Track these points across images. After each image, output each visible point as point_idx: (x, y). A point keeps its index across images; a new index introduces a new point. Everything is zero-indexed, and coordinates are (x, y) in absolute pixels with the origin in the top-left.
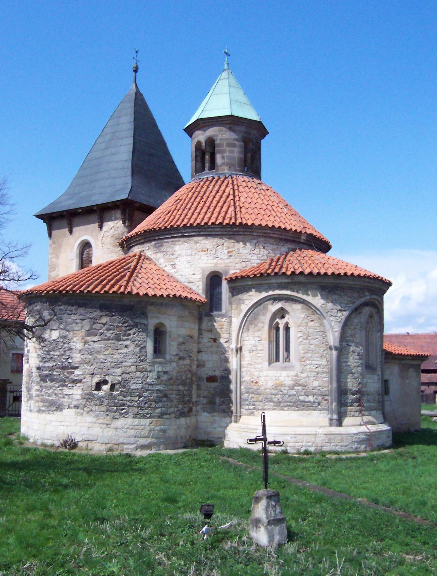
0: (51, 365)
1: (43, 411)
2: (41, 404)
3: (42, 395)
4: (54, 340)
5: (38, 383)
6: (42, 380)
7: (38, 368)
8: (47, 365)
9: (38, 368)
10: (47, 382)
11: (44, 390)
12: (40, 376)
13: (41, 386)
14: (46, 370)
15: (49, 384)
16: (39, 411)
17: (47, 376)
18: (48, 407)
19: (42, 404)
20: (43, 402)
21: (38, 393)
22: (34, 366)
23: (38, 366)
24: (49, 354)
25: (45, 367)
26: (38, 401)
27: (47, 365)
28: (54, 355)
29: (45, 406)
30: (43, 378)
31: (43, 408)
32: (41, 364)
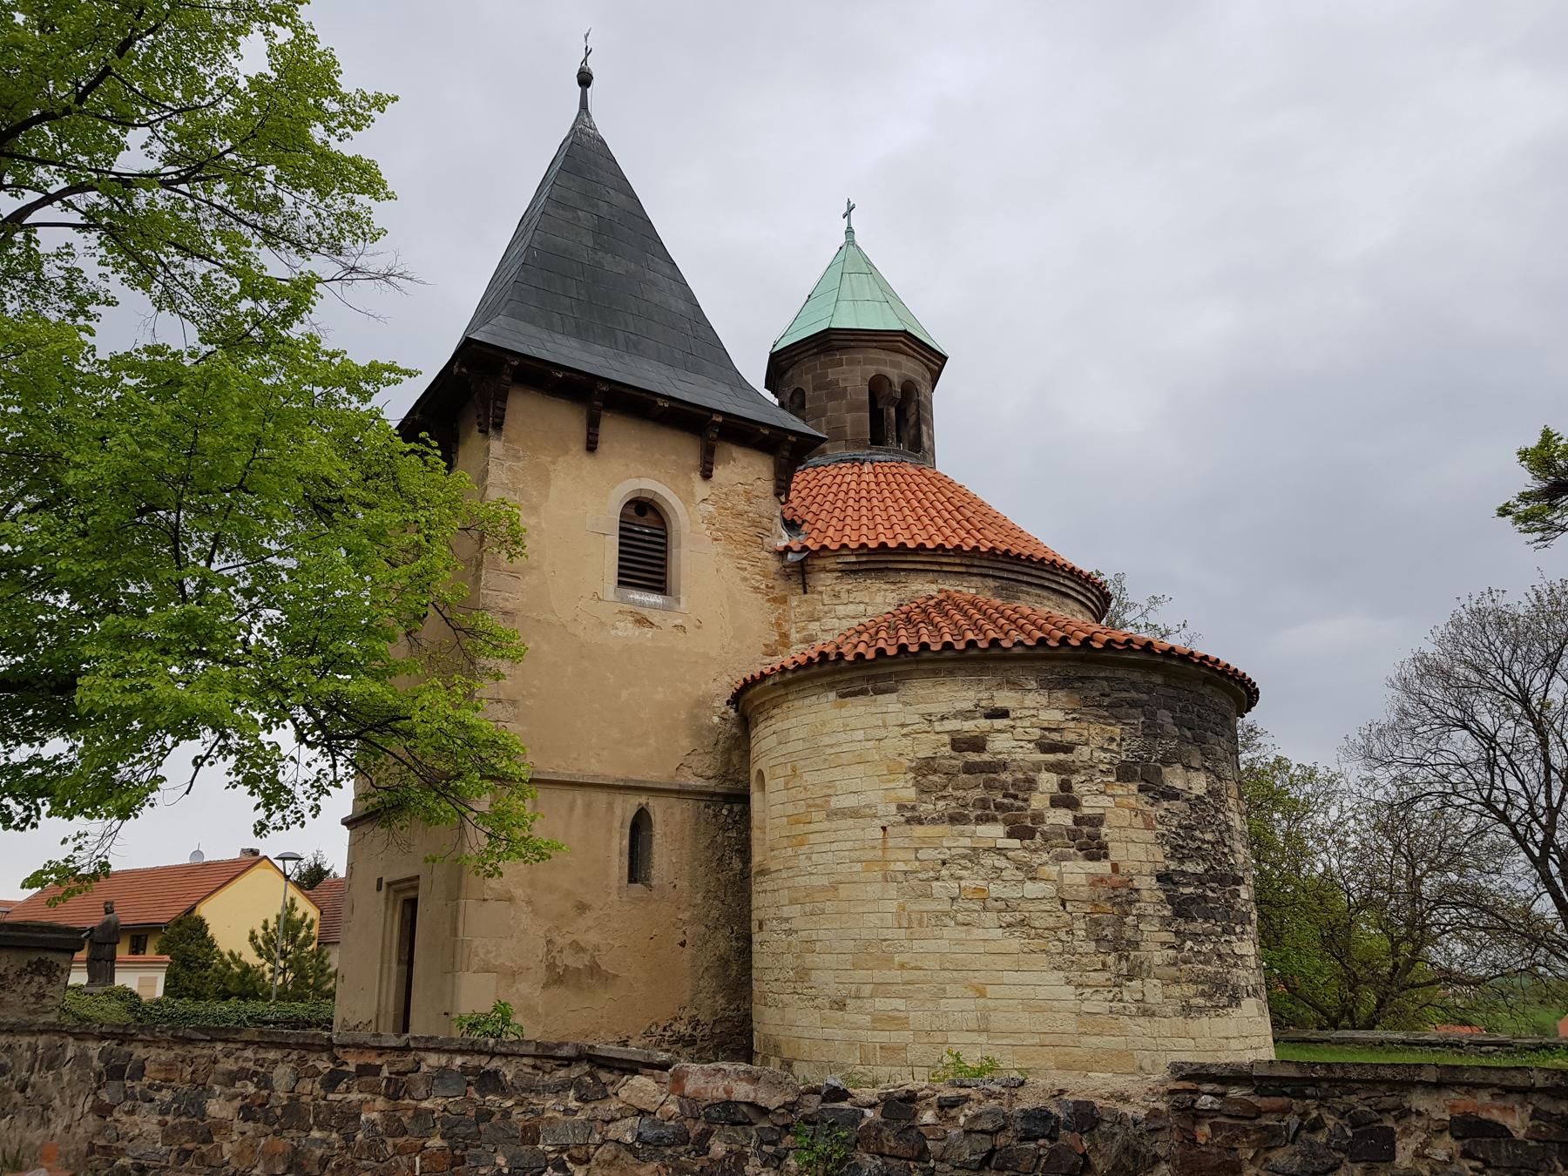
0: (1200, 869)
1: (1200, 1010)
2: (1189, 990)
4: (1198, 797)
5: (1166, 923)
6: (1178, 914)
7: (1163, 878)
8: (1190, 867)
10: (1194, 919)
11: (1189, 943)
13: (1177, 933)
14: (1188, 885)
15: (1199, 926)
16: (1187, 1010)
17: (1192, 899)
18: (1210, 997)
20: (1196, 983)
21: (1172, 952)
22: (1147, 868)
24: (1194, 839)
25: (1183, 873)
26: (1177, 981)
27: (1190, 867)
28: (1204, 841)
29: (1203, 994)
30: (1182, 909)
31: (1201, 1001)
32: (1173, 865)
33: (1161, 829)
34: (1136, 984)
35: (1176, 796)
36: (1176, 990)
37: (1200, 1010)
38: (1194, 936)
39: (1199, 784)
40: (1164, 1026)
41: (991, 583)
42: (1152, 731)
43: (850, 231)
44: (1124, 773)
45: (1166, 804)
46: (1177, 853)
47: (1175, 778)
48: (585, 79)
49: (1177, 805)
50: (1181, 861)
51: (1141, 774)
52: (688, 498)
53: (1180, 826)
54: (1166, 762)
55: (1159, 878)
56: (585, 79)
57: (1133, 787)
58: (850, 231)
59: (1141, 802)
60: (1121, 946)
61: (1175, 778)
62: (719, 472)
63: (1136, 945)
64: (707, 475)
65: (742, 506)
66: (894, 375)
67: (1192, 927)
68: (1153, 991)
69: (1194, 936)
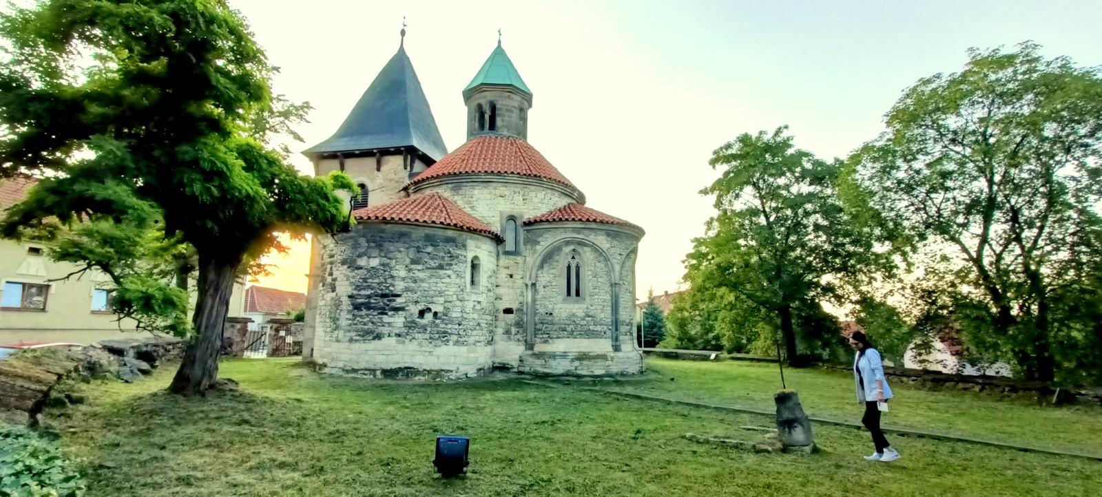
1: (356, 341)
3: (356, 324)
5: (349, 312)
8: (363, 292)
9: (350, 297)
12: (353, 304)
13: (353, 315)
15: (364, 312)
16: (351, 340)
17: (362, 304)
18: (363, 336)
19: (355, 333)
22: (345, 294)
23: (350, 294)
24: (366, 282)
25: (359, 295)
26: (349, 331)
27: (363, 292)
29: (359, 335)
30: (357, 307)
31: (357, 338)
32: (355, 292)
33: (353, 280)
34: (336, 332)
35: (361, 268)
36: (348, 334)
37: (356, 341)
38: (361, 316)
39: (375, 262)
40: (342, 345)
41: (450, 186)
42: (356, 246)
43: (499, 42)
44: (343, 262)
45: (356, 271)
46: (358, 288)
47: (362, 262)
48: (403, 33)
49: (360, 272)
50: (360, 290)
51: (350, 263)
52: (372, 180)
53: (361, 278)
54: (360, 256)
55: (349, 297)
56: (403, 33)
57: (346, 267)
58: (499, 42)
59: (348, 272)
60: (335, 320)
61: (362, 262)
62: (383, 168)
63: (338, 319)
64: (378, 170)
65: (393, 176)
66: (483, 102)
67: (360, 313)
68: (341, 334)
69: (361, 316)
